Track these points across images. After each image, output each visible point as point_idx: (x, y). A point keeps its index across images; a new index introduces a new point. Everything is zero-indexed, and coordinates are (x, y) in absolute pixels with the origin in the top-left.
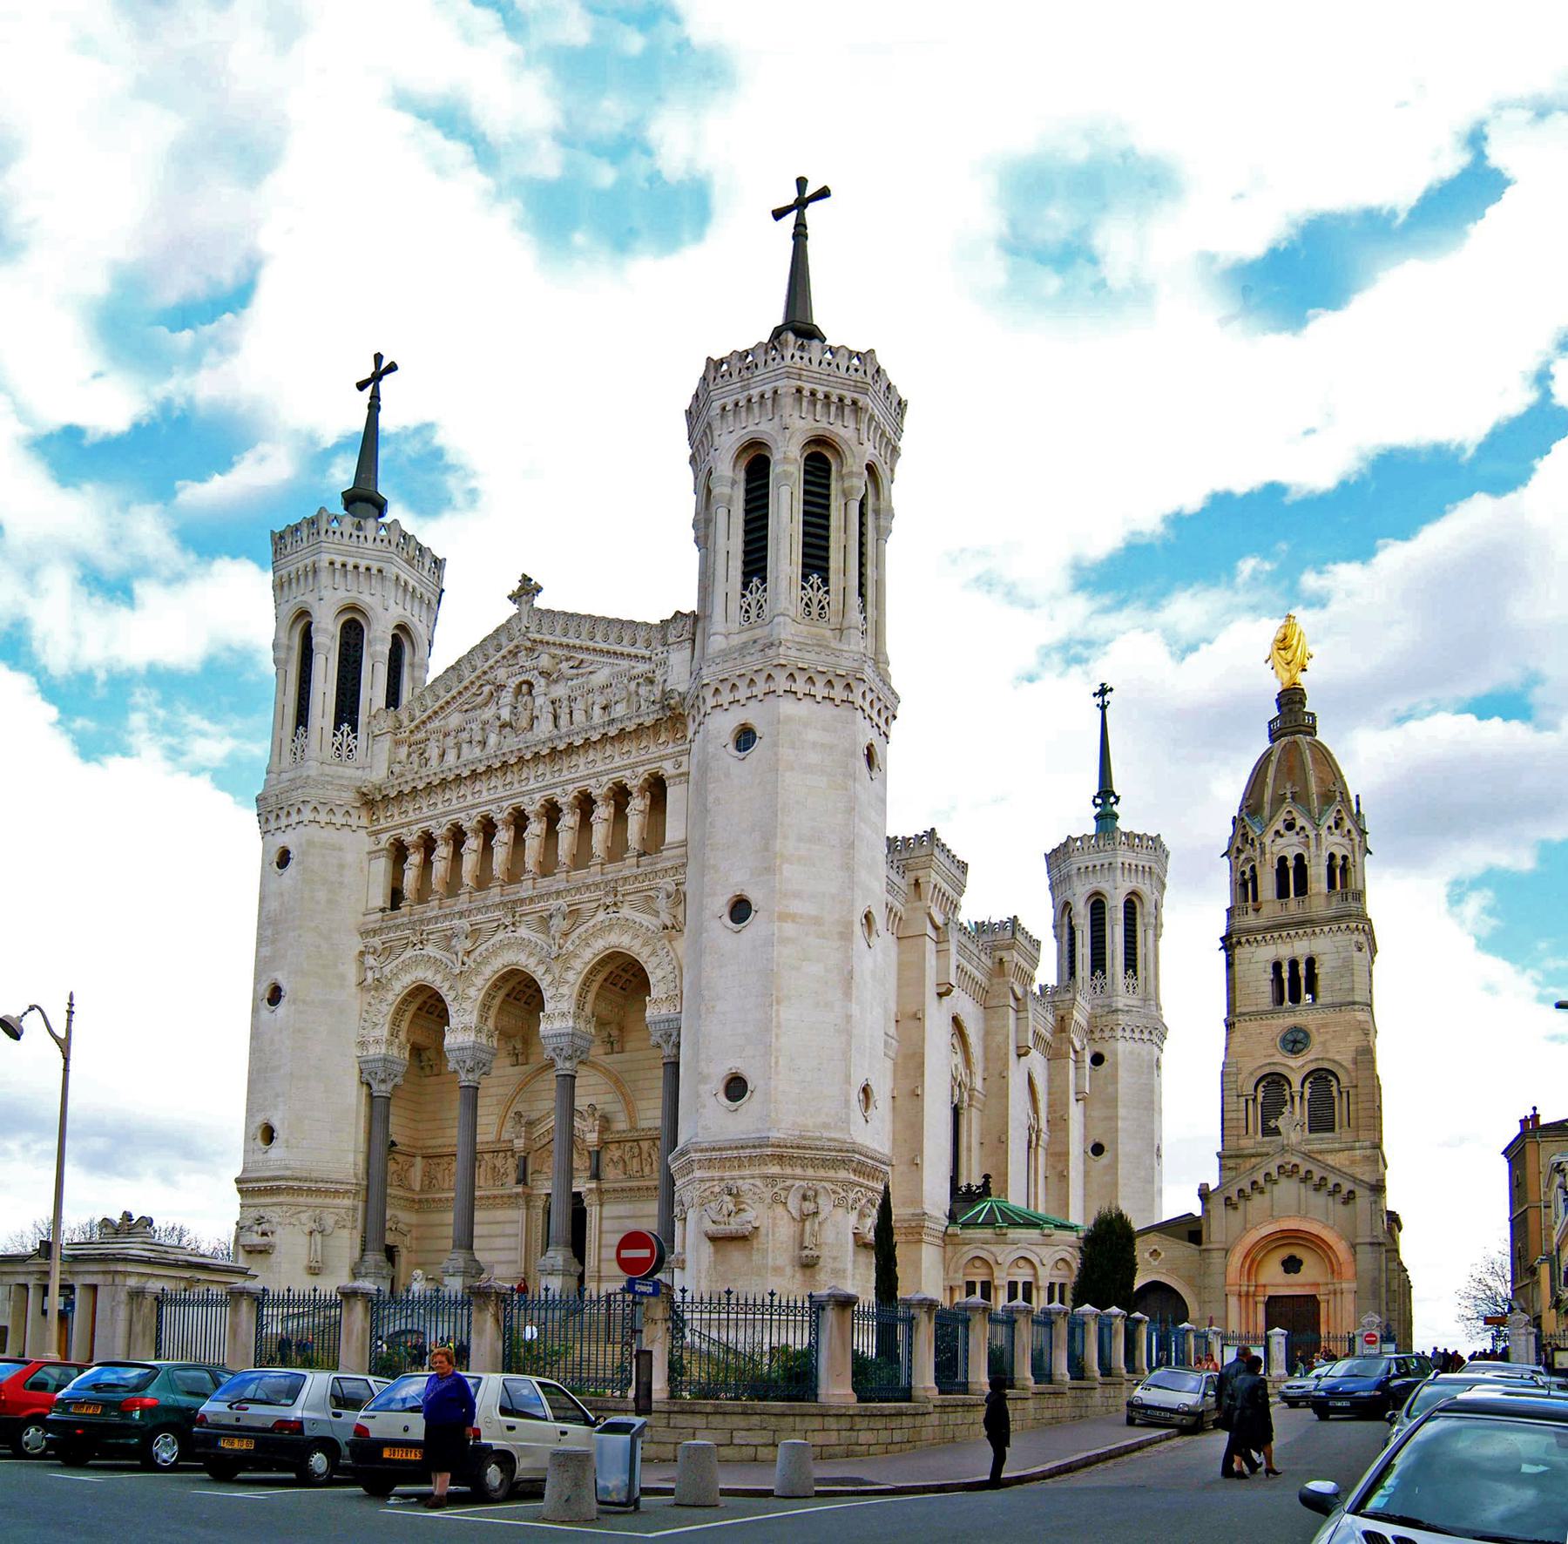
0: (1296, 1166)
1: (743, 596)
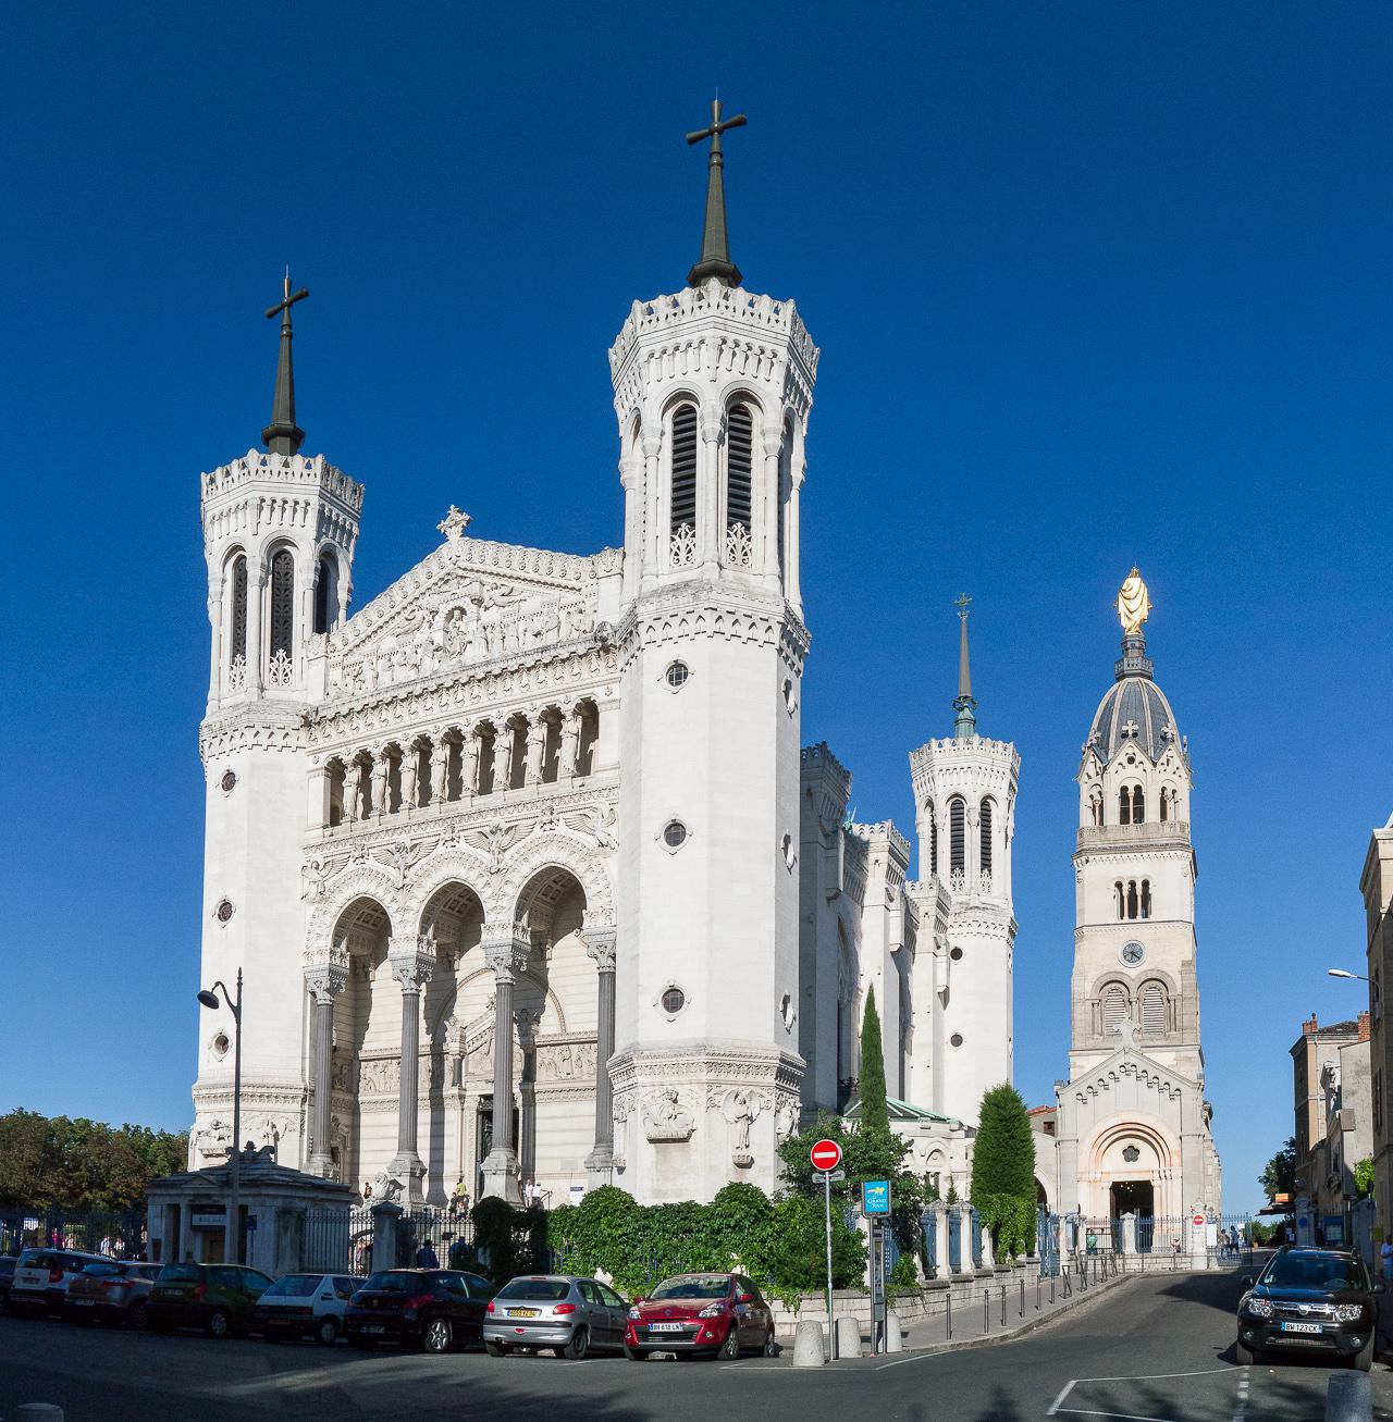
1: (673, 540)
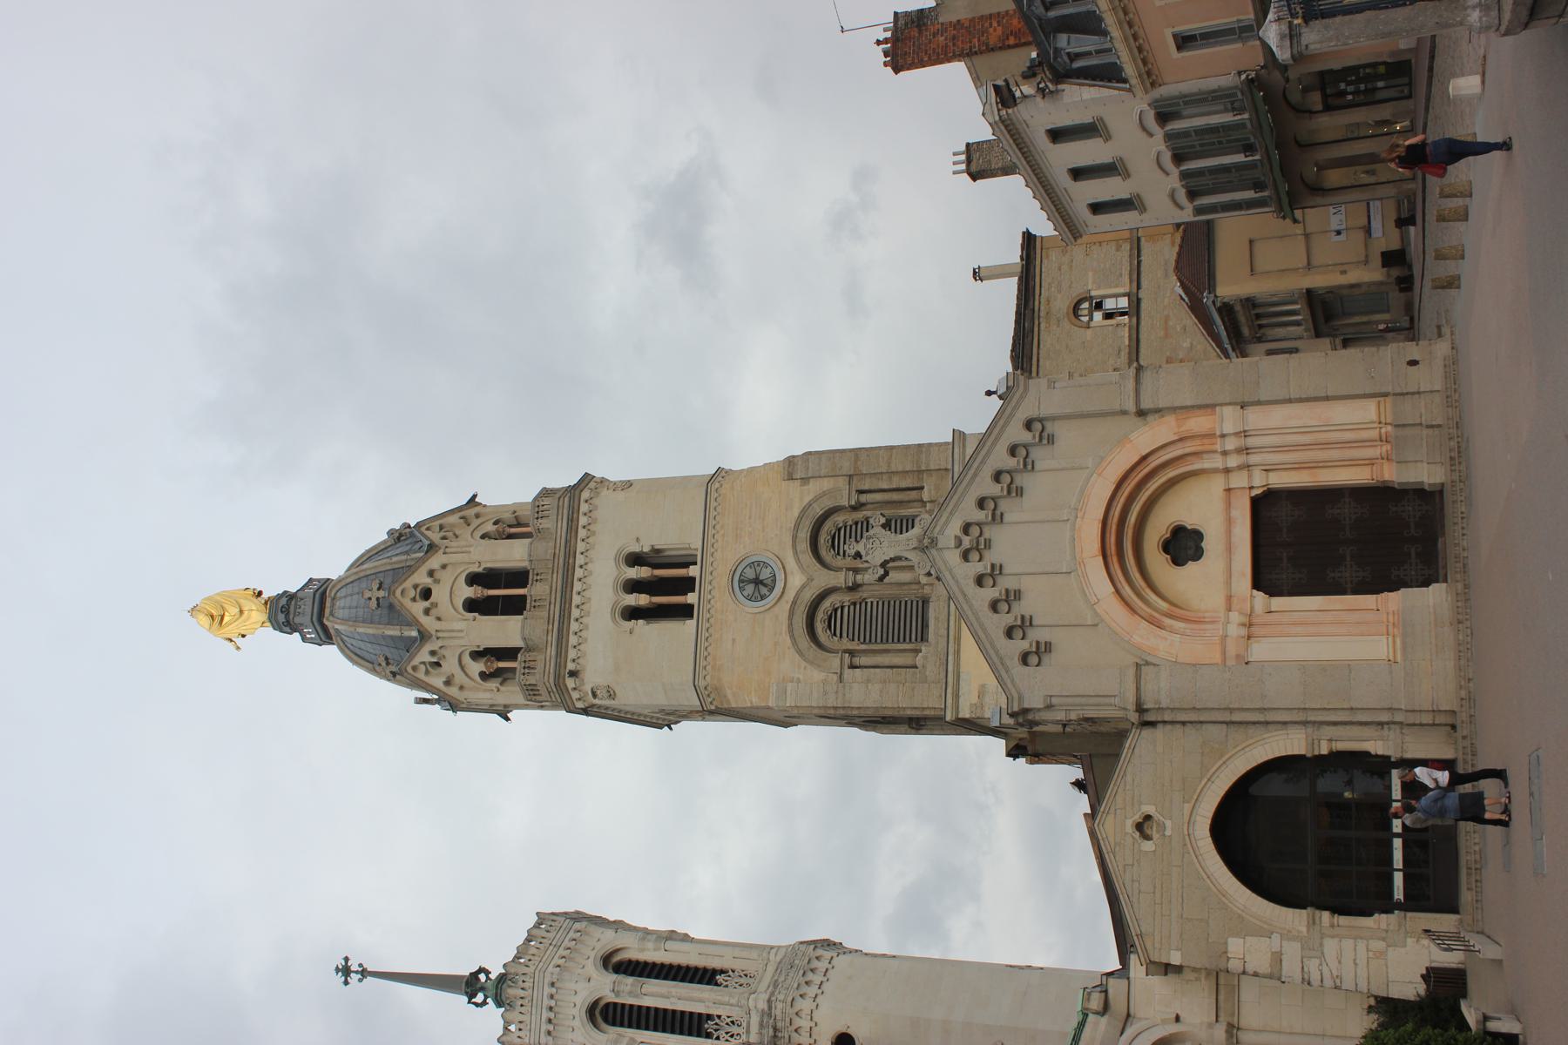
0: (966, 529)
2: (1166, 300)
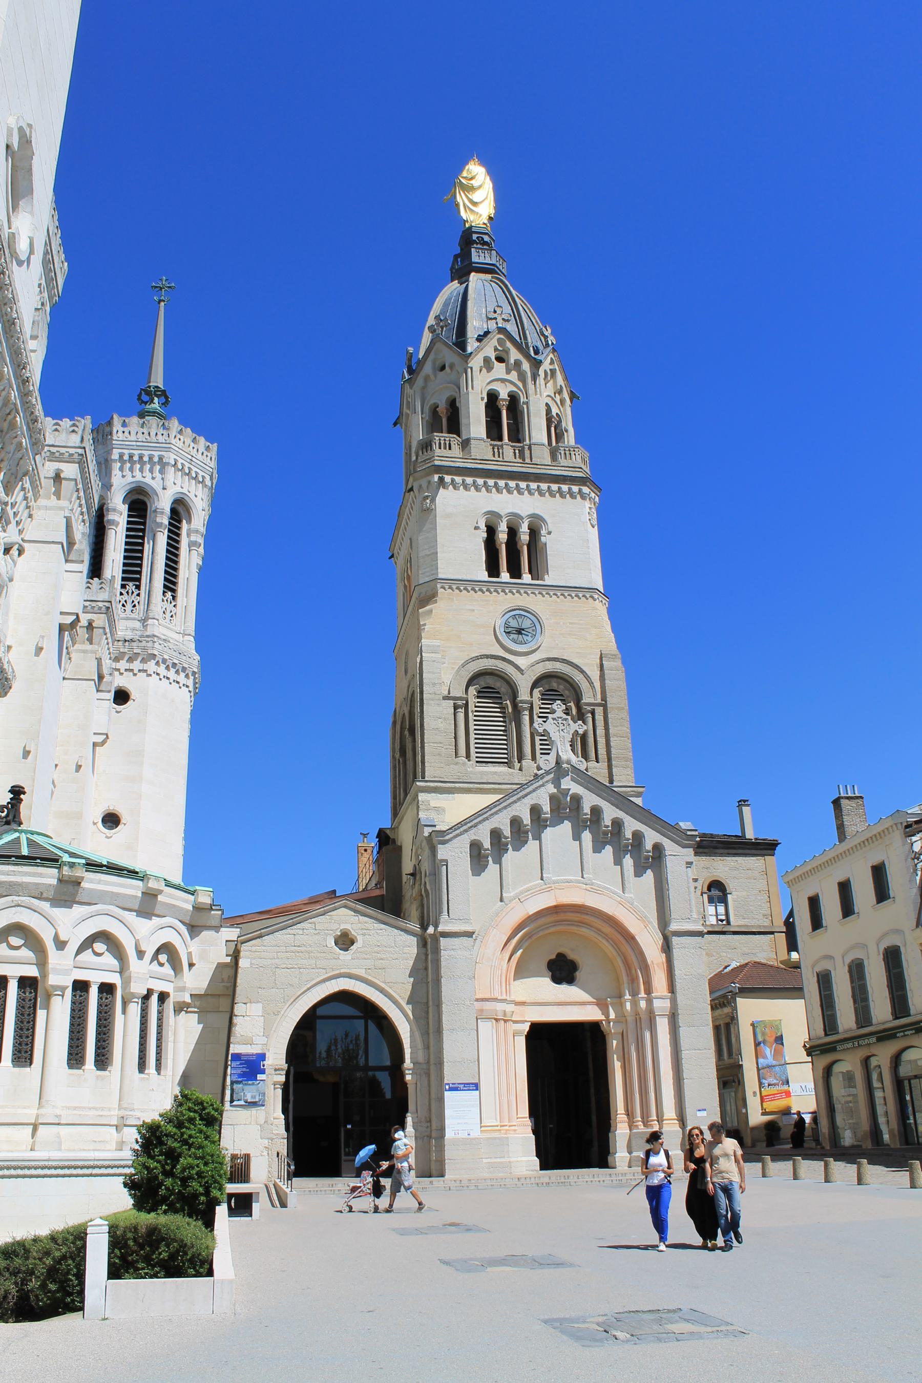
0: (577, 799)
2: (725, 954)
